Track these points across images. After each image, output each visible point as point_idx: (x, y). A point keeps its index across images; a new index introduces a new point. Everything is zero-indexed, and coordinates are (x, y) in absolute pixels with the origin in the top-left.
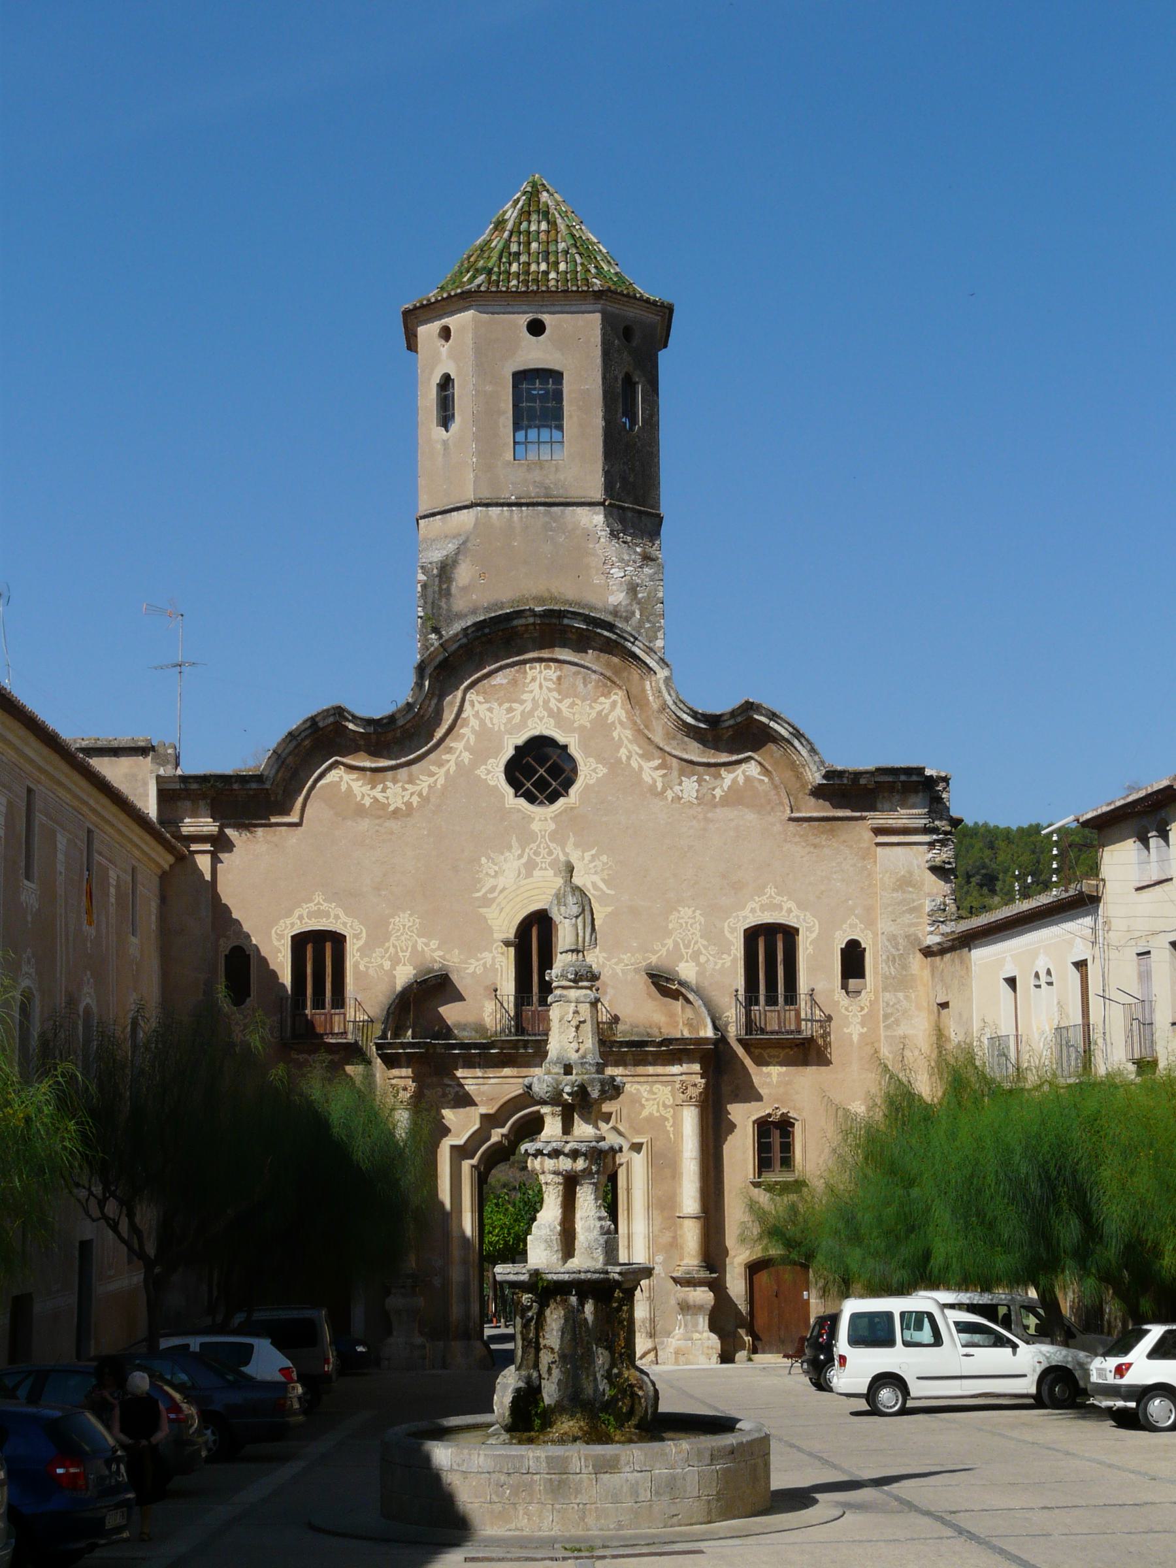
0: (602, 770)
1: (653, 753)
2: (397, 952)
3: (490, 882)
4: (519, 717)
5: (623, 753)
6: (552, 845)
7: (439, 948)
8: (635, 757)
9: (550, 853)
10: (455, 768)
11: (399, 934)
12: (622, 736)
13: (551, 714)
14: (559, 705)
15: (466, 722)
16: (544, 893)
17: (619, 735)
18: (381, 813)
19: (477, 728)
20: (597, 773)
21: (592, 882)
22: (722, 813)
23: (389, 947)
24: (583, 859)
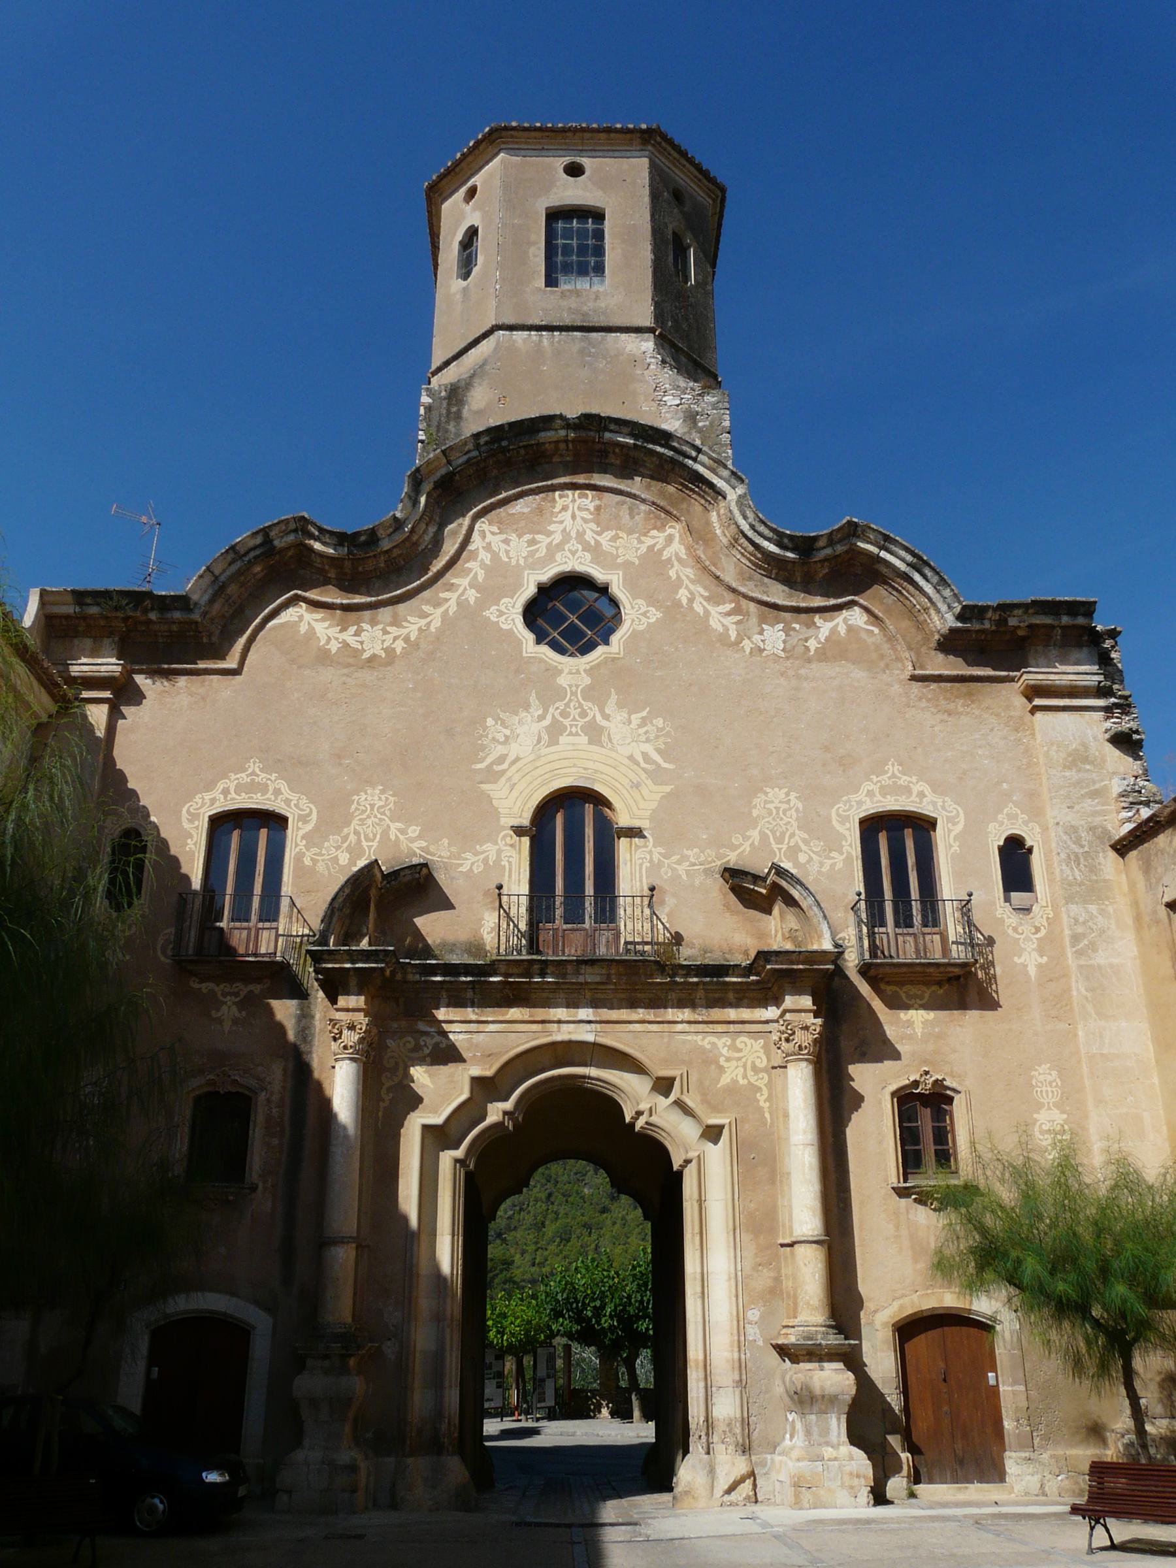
0: (655, 615)
1: (722, 595)
3: (500, 750)
4: (545, 550)
5: (683, 595)
6: (587, 705)
7: (420, 837)
8: (699, 599)
9: (584, 714)
10: (455, 609)
11: (364, 816)
12: (681, 574)
13: (587, 547)
14: (598, 538)
15: (474, 555)
16: (575, 766)
17: (677, 573)
18: (351, 660)
19: (488, 562)
20: (648, 618)
21: (642, 753)
22: (817, 669)
23: (348, 834)
24: (630, 722)
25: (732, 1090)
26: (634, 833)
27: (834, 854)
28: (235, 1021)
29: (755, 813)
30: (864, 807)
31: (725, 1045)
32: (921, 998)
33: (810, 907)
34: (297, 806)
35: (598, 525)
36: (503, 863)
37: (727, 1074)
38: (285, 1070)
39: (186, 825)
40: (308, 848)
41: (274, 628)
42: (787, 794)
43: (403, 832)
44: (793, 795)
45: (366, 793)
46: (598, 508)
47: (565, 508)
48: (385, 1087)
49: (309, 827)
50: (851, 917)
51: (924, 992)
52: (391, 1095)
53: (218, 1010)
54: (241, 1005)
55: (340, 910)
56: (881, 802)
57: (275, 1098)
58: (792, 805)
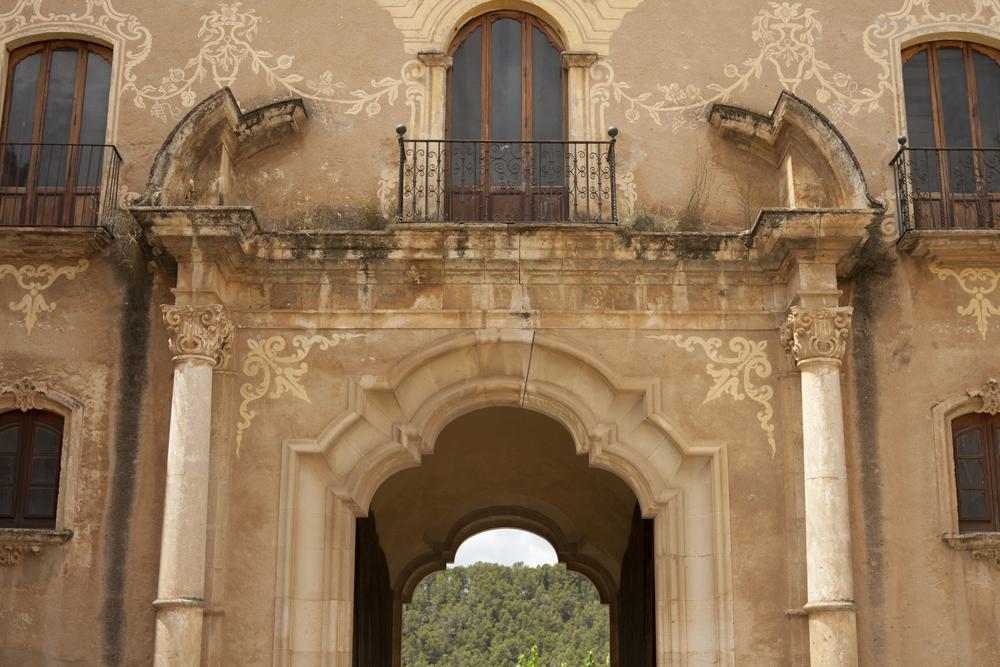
2: (210, 75)
7: (293, 69)
11: (217, 43)
25: (724, 406)
26: (586, 59)
27: (865, 92)
28: (42, 316)
29: (756, 36)
30: (908, 28)
31: (714, 348)
32: (987, 285)
33: (834, 154)
34: (124, 29)
36: (407, 103)
37: (716, 387)
38: (109, 380)
42: (801, 11)
43: (270, 63)
44: (809, 13)
45: (220, 12)
48: (245, 403)
49: (141, 58)
50: (890, 178)
51: (990, 278)
52: (253, 413)
53: (18, 301)
54: (50, 294)
55: (179, 158)
56: (931, 21)
57: (96, 417)
58: (807, 26)
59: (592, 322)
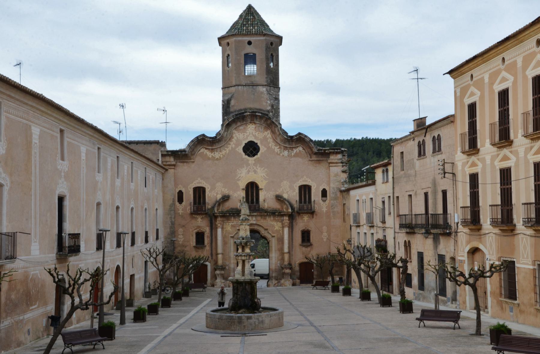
0: (265, 149)
3: (239, 175)
5: (270, 145)
6: (254, 167)
7: (227, 191)
9: (253, 168)
13: (253, 136)
22: (293, 159)
25: (276, 230)
26: (261, 189)
28: (201, 221)
29: (282, 185)
35: (255, 131)
39: (189, 190)
40: (209, 193)
41: (200, 153)
43: (225, 190)
44: (288, 182)
46: (255, 127)
47: (249, 127)
54: (201, 219)
57: (208, 233)
59: (262, 221)
